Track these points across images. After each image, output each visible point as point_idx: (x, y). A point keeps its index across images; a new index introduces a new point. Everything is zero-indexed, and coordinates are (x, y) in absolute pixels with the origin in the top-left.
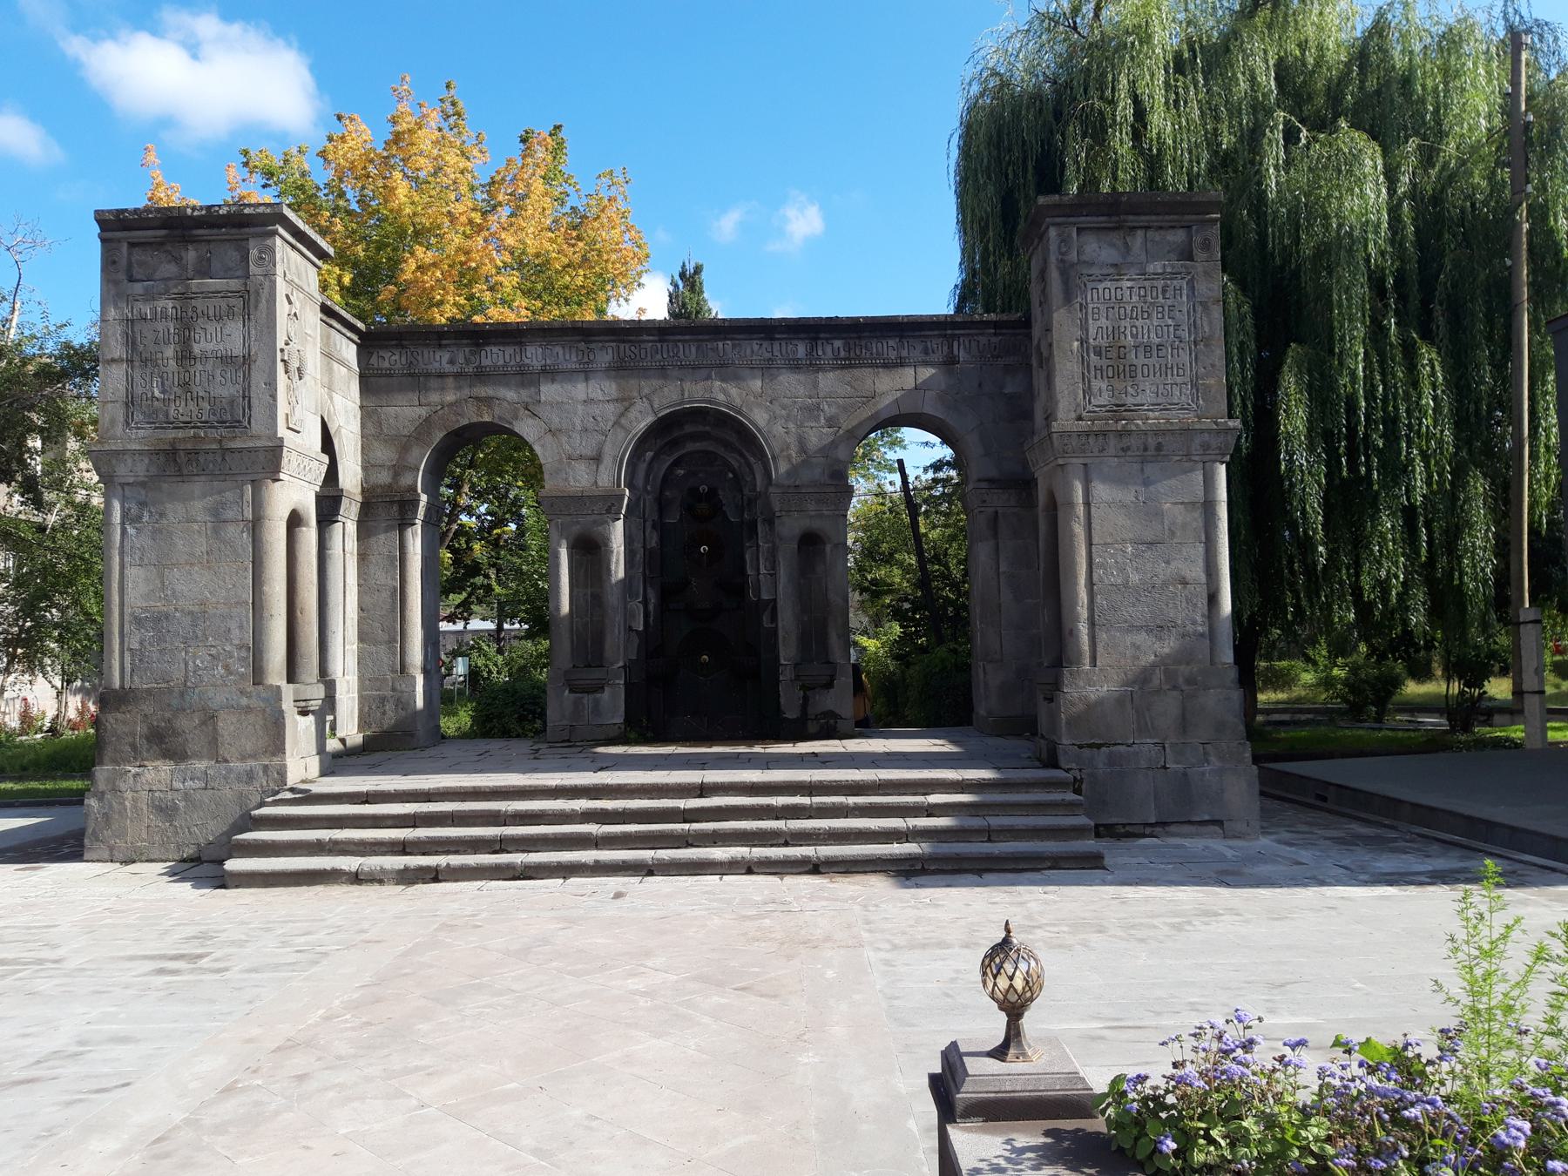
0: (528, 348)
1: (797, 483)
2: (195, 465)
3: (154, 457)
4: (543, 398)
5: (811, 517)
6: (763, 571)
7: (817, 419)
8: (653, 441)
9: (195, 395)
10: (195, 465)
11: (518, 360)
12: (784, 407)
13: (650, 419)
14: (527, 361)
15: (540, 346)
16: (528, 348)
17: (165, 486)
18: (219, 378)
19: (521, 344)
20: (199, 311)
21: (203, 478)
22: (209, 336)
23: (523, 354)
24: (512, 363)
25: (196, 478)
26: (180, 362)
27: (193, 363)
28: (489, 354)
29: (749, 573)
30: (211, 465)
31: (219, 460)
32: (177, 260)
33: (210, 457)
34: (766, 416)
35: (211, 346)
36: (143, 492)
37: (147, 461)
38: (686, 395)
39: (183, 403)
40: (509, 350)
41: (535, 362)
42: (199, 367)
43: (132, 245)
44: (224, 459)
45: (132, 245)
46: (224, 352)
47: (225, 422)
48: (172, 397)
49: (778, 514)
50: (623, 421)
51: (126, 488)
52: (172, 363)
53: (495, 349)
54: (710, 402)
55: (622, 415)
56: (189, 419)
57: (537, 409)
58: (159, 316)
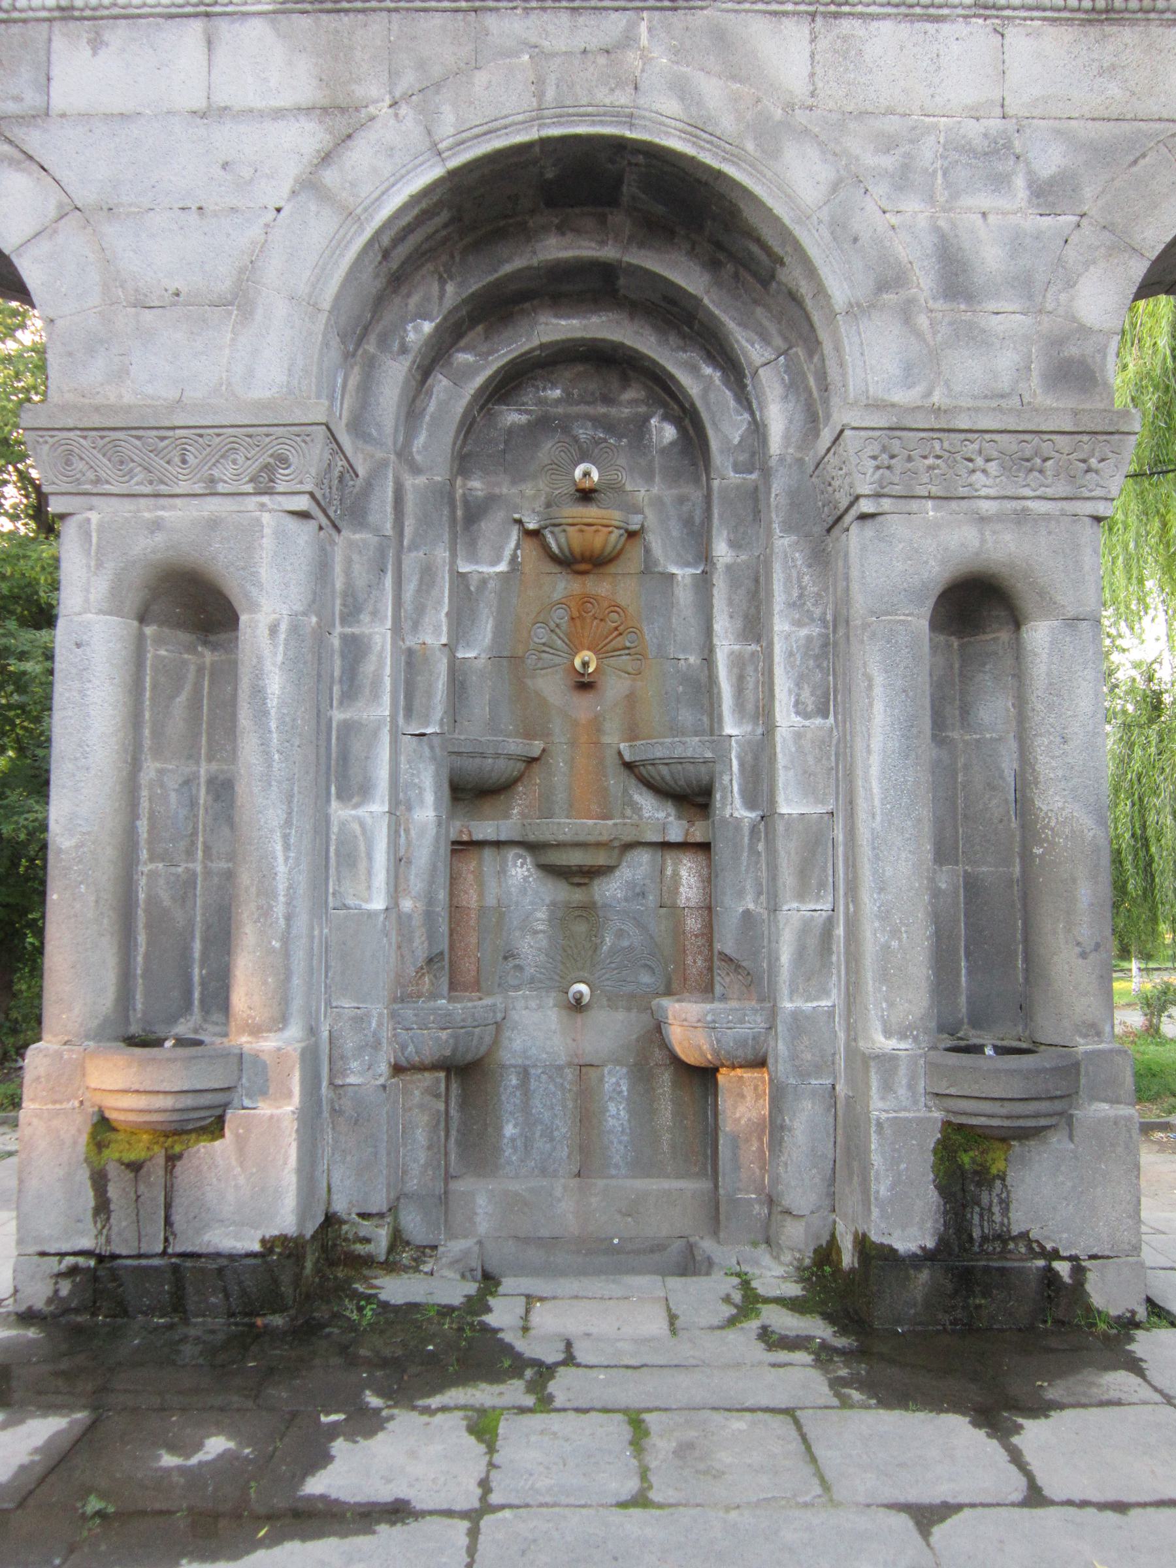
1: (937, 398)
4: (58, 102)
5: (983, 520)
6: (786, 718)
7: (1000, 182)
8: (435, 287)
12: (887, 144)
13: (432, 173)
29: (730, 728)
34: (825, 173)
38: (550, 94)
49: (866, 506)
50: (330, 177)
54: (630, 120)
55: (326, 158)
57: (33, 140)
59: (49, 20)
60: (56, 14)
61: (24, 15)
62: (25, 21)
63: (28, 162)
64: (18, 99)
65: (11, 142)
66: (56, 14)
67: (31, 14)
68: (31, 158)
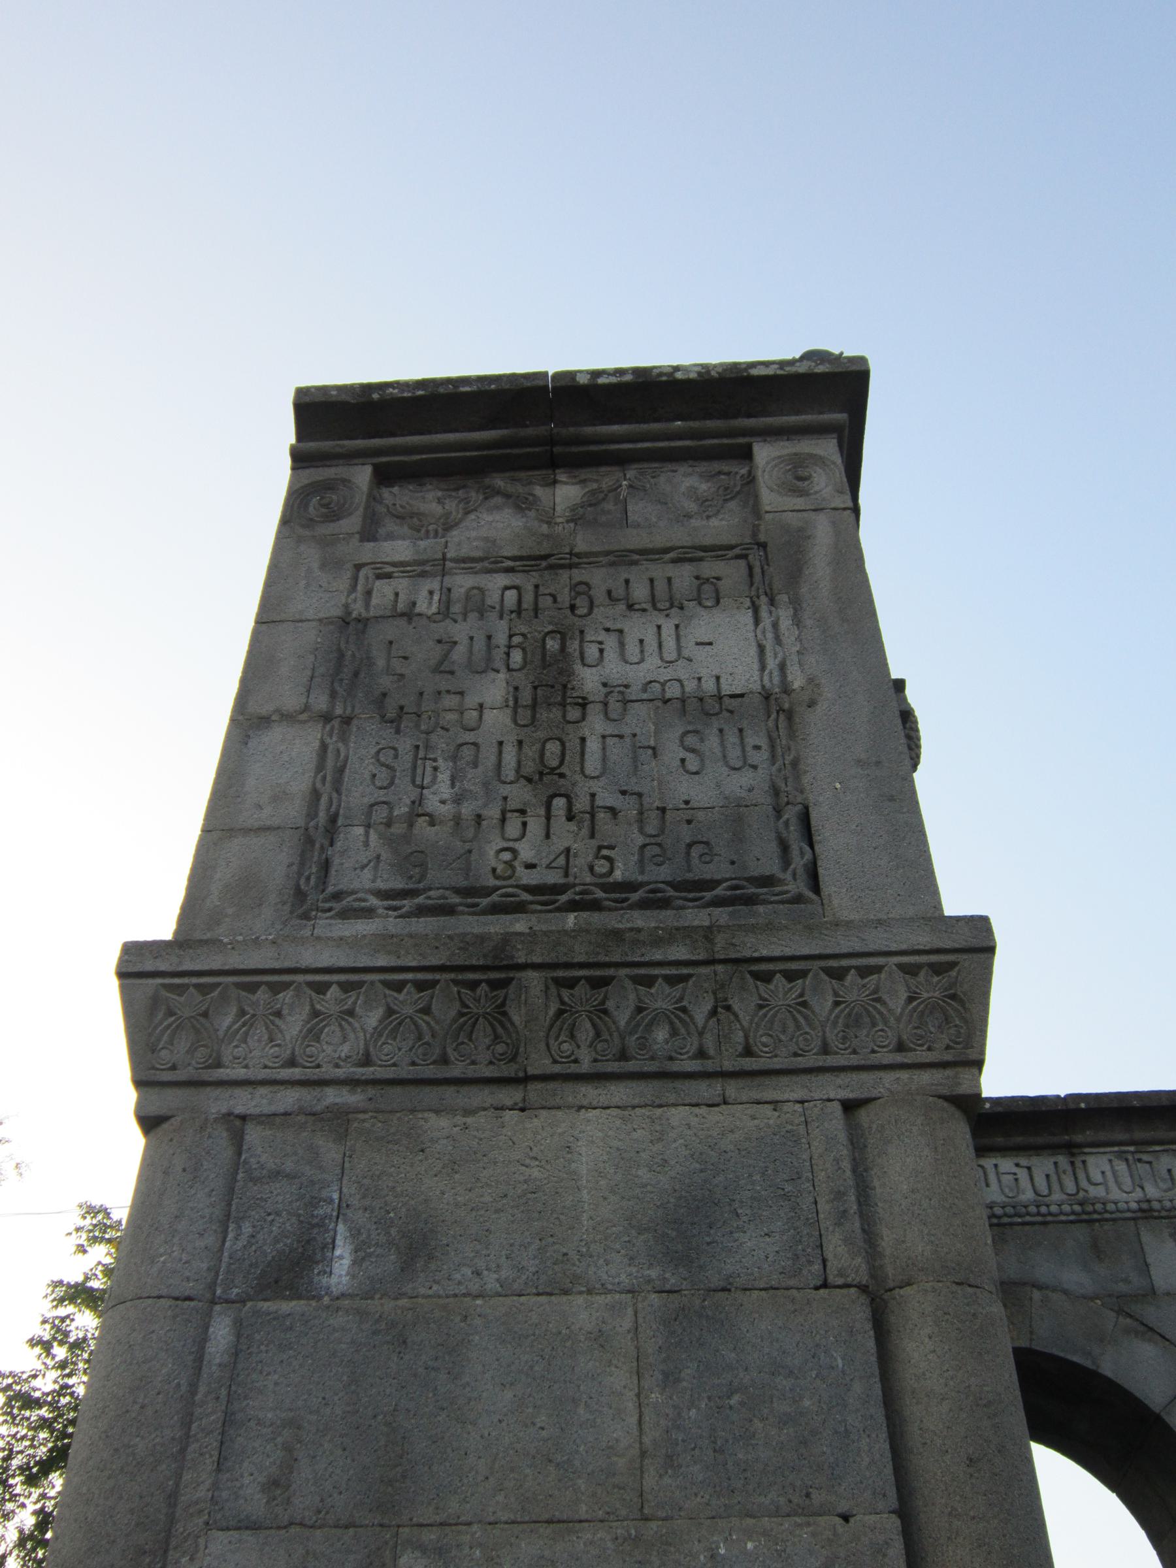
0: (1091, 1160)
2: (585, 1032)
3: (407, 1001)
9: (581, 804)
10: (585, 1032)
11: (1070, 1187)
14: (1096, 1192)
15: (1121, 1155)
16: (1091, 1160)
17: (438, 1125)
18: (672, 752)
19: (1071, 1149)
20: (599, 594)
21: (619, 1092)
22: (632, 650)
23: (1081, 1176)
24: (1057, 1196)
25: (589, 1092)
26: (524, 716)
27: (574, 714)
28: (992, 1177)
30: (661, 1034)
31: (700, 1012)
32: (522, 504)
33: (661, 998)
35: (637, 675)
36: (331, 1152)
37: (373, 1019)
39: (535, 826)
40: (1043, 1165)
41: (1116, 1194)
42: (596, 724)
43: (384, 476)
44: (720, 1008)
45: (384, 476)
46: (690, 686)
47: (711, 884)
48: (494, 812)
51: (254, 1135)
52: (497, 722)
53: (1006, 1164)
56: (554, 878)
57: (1150, 1313)
58: (456, 608)
59: (1134, 1219)
60: (1139, 1214)
61: (1114, 1216)
62: (1114, 1220)
63: (1150, 1333)
64: (1126, 1281)
65: (1131, 1316)
66: (1139, 1214)
67: (1119, 1215)
68: (1151, 1329)
